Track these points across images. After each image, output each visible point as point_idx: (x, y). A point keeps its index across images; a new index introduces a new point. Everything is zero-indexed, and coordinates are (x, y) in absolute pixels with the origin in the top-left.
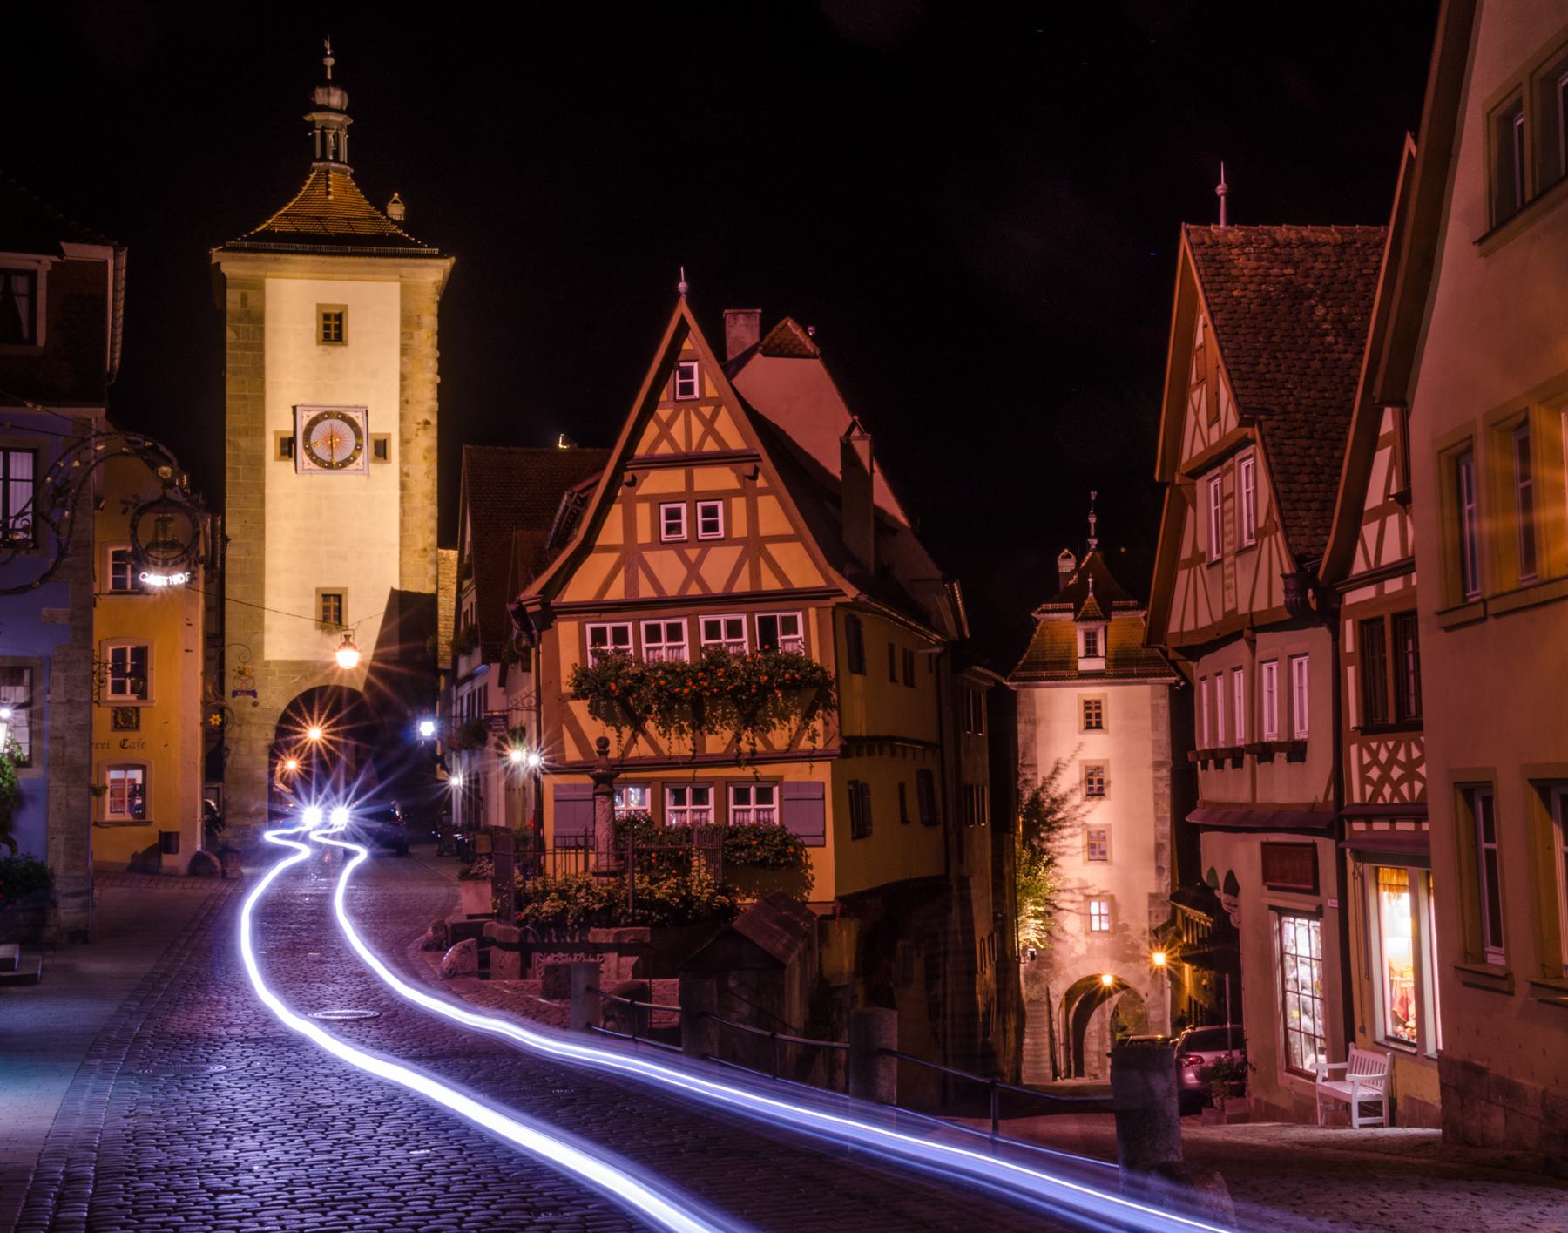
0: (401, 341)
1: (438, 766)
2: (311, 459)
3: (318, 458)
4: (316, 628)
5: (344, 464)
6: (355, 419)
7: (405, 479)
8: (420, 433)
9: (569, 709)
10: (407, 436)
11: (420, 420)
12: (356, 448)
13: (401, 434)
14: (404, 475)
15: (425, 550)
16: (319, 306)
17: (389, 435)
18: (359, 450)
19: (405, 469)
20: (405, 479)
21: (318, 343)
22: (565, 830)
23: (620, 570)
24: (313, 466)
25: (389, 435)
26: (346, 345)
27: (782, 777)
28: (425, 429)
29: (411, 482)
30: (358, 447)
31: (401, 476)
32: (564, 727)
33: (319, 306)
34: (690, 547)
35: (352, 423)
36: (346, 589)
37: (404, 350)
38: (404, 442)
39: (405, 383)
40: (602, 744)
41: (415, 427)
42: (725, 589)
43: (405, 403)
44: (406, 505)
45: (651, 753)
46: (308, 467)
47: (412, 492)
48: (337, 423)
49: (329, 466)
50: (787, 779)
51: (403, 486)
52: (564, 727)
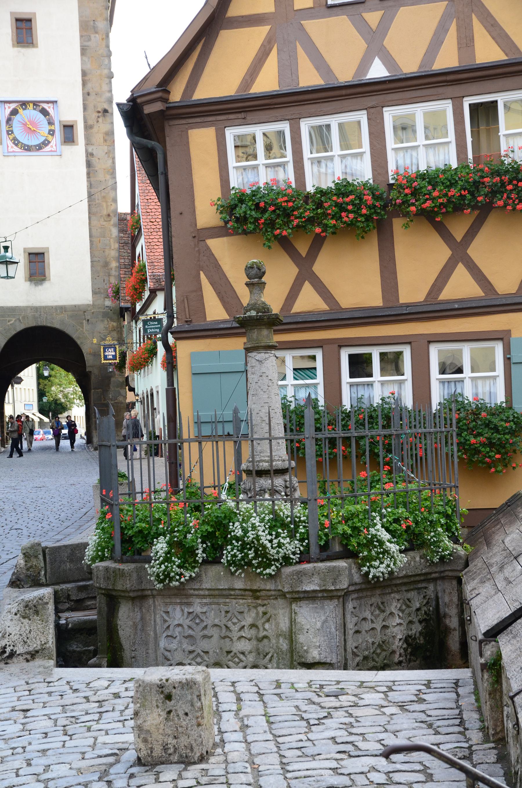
0: (81, 43)
1: (127, 388)
2: (14, 143)
3: (19, 142)
4: (26, 281)
5: (40, 147)
6: (48, 109)
7: (90, 158)
8: (100, 120)
9: (208, 248)
10: (90, 122)
11: (100, 110)
12: (49, 133)
13: (85, 122)
14: (89, 155)
15: (109, 215)
16: (12, 13)
17: (76, 121)
18: (53, 135)
19: (90, 150)
20: (90, 158)
21: (14, 46)
22: (206, 415)
23: (270, 50)
24: (16, 149)
25: (76, 121)
26: (37, 47)
27: (509, 332)
28: (104, 116)
29: (94, 160)
30: (52, 133)
31: (87, 156)
32: (202, 275)
33: (12, 13)
34: (370, 10)
35: (45, 112)
36: (48, 248)
37: (84, 51)
38: (88, 127)
39: (86, 78)
40: (254, 272)
41: (97, 114)
42: (420, 67)
43: (86, 95)
44: (92, 179)
45: (323, 306)
46: (12, 150)
47: (96, 168)
48: (31, 113)
49: (28, 148)
50: (514, 335)
51: (89, 164)
52: (202, 275)
